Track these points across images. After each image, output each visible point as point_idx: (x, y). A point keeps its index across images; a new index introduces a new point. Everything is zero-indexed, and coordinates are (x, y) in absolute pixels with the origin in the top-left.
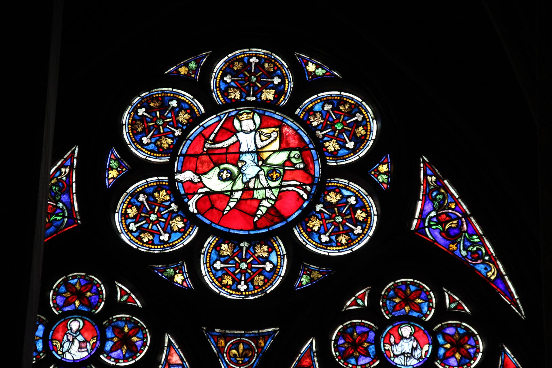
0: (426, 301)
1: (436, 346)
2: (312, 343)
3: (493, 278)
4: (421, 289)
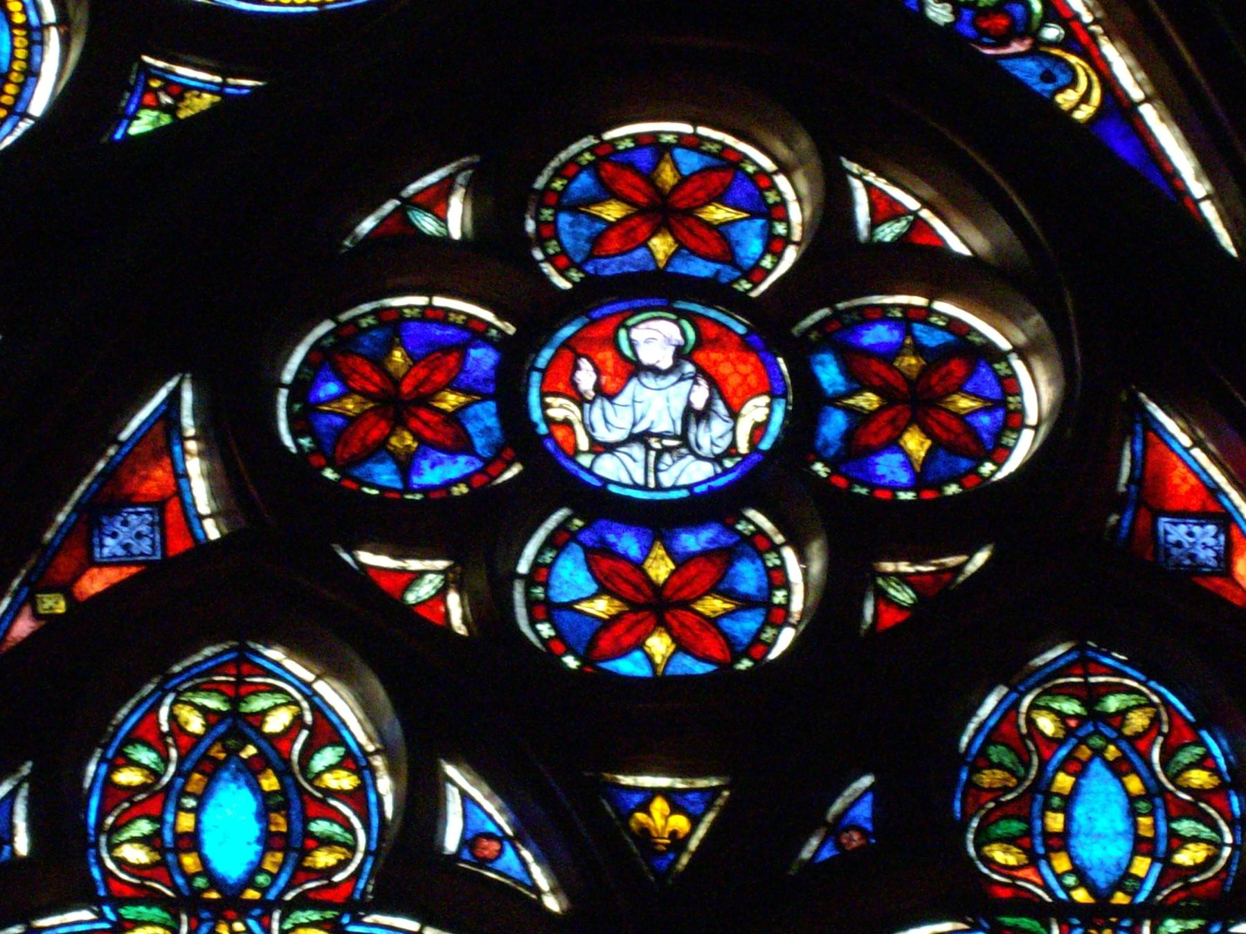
0: (753, 216)
1: (807, 404)
2: (175, 396)
3: (1083, 114)
4: (729, 161)
